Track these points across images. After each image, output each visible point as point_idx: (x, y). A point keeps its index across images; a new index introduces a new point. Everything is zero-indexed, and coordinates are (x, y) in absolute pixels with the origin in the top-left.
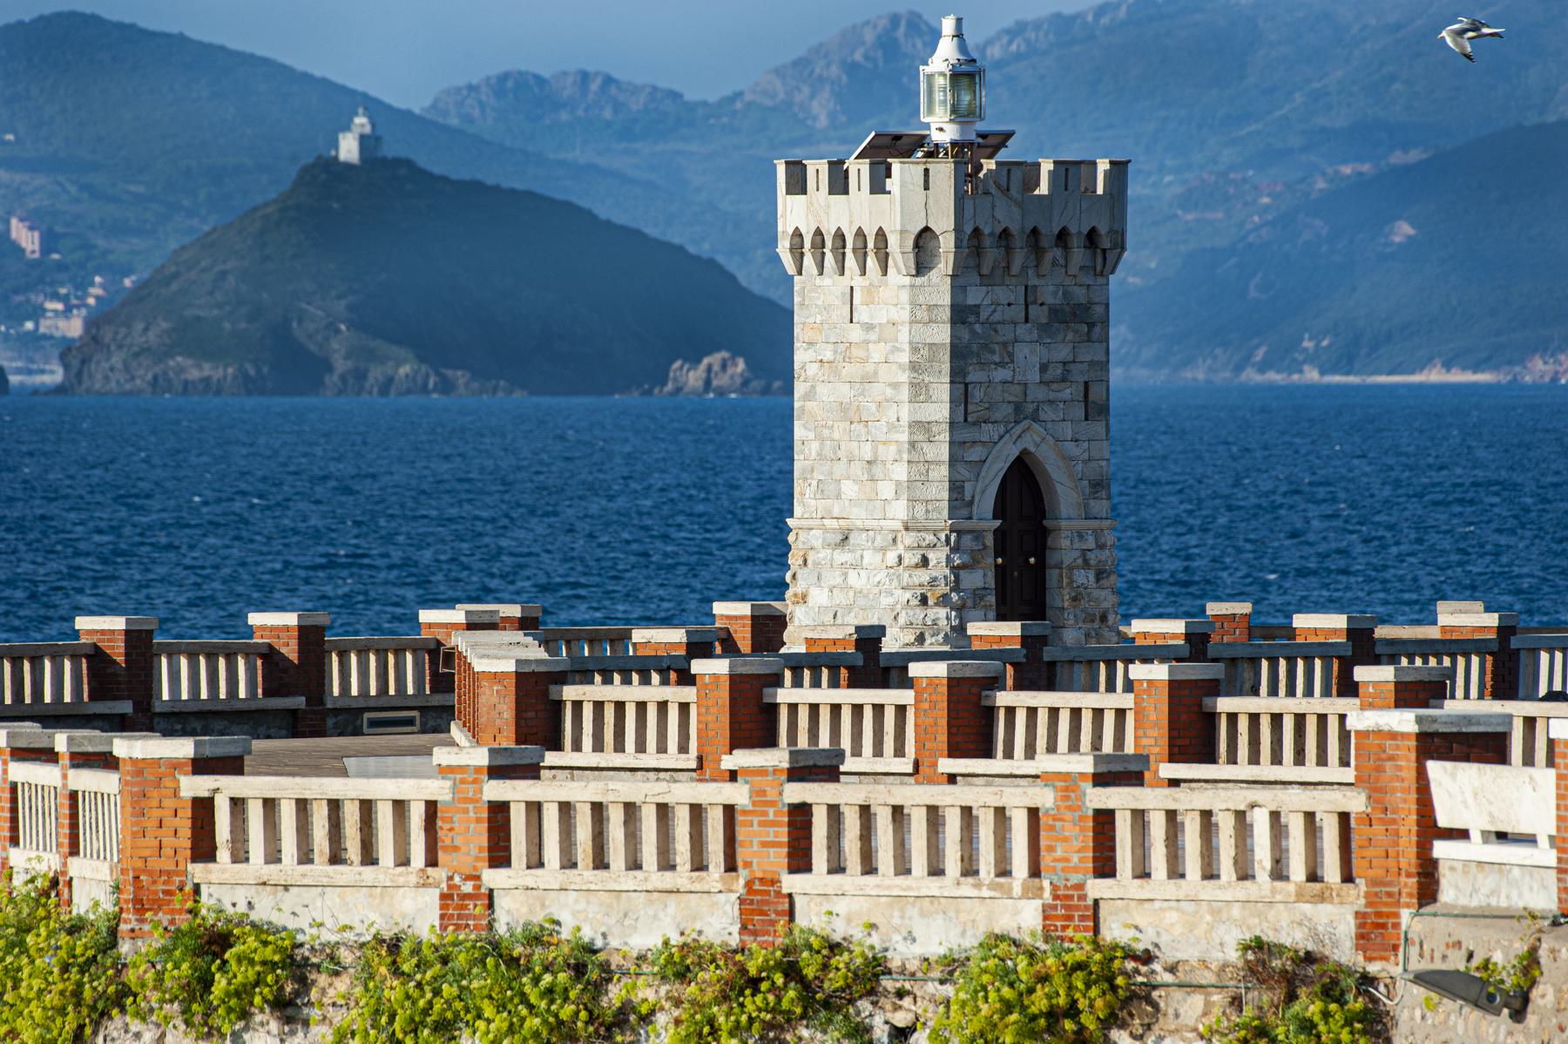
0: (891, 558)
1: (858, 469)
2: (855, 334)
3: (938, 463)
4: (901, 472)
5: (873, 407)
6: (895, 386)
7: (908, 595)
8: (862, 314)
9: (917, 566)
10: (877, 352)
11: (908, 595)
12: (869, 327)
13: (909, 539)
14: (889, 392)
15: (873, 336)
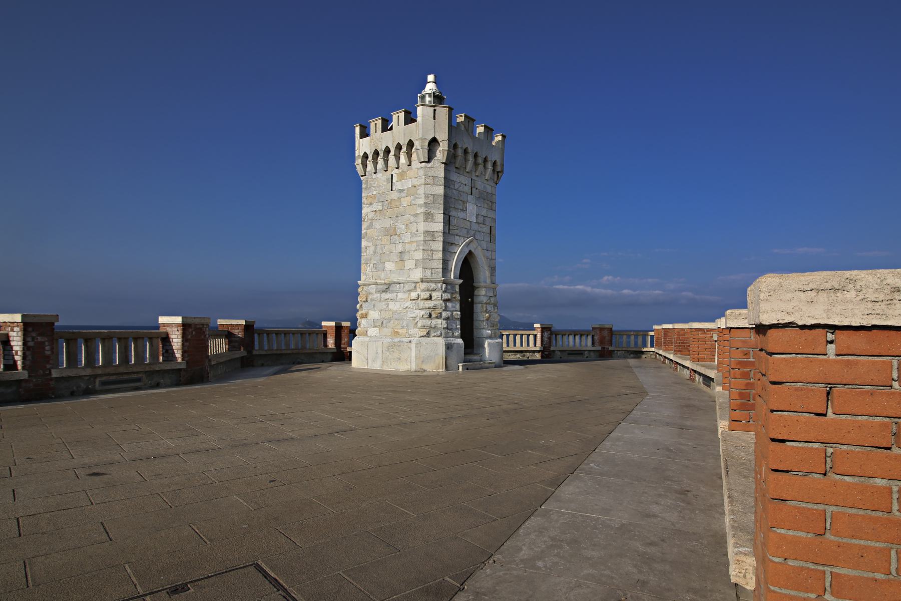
0: (414, 295)
1: (394, 257)
2: (394, 195)
3: (438, 251)
4: (419, 255)
5: (403, 227)
6: (416, 215)
7: (423, 312)
8: (397, 185)
9: (427, 299)
10: (405, 202)
11: (423, 312)
12: (401, 191)
13: (424, 286)
14: (412, 219)
15: (403, 195)
